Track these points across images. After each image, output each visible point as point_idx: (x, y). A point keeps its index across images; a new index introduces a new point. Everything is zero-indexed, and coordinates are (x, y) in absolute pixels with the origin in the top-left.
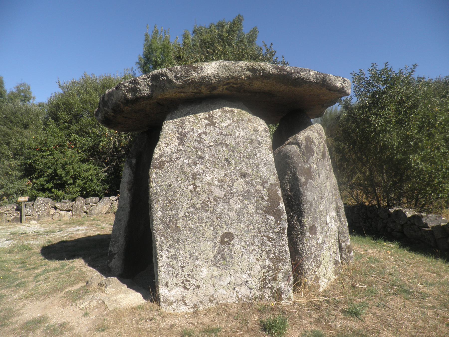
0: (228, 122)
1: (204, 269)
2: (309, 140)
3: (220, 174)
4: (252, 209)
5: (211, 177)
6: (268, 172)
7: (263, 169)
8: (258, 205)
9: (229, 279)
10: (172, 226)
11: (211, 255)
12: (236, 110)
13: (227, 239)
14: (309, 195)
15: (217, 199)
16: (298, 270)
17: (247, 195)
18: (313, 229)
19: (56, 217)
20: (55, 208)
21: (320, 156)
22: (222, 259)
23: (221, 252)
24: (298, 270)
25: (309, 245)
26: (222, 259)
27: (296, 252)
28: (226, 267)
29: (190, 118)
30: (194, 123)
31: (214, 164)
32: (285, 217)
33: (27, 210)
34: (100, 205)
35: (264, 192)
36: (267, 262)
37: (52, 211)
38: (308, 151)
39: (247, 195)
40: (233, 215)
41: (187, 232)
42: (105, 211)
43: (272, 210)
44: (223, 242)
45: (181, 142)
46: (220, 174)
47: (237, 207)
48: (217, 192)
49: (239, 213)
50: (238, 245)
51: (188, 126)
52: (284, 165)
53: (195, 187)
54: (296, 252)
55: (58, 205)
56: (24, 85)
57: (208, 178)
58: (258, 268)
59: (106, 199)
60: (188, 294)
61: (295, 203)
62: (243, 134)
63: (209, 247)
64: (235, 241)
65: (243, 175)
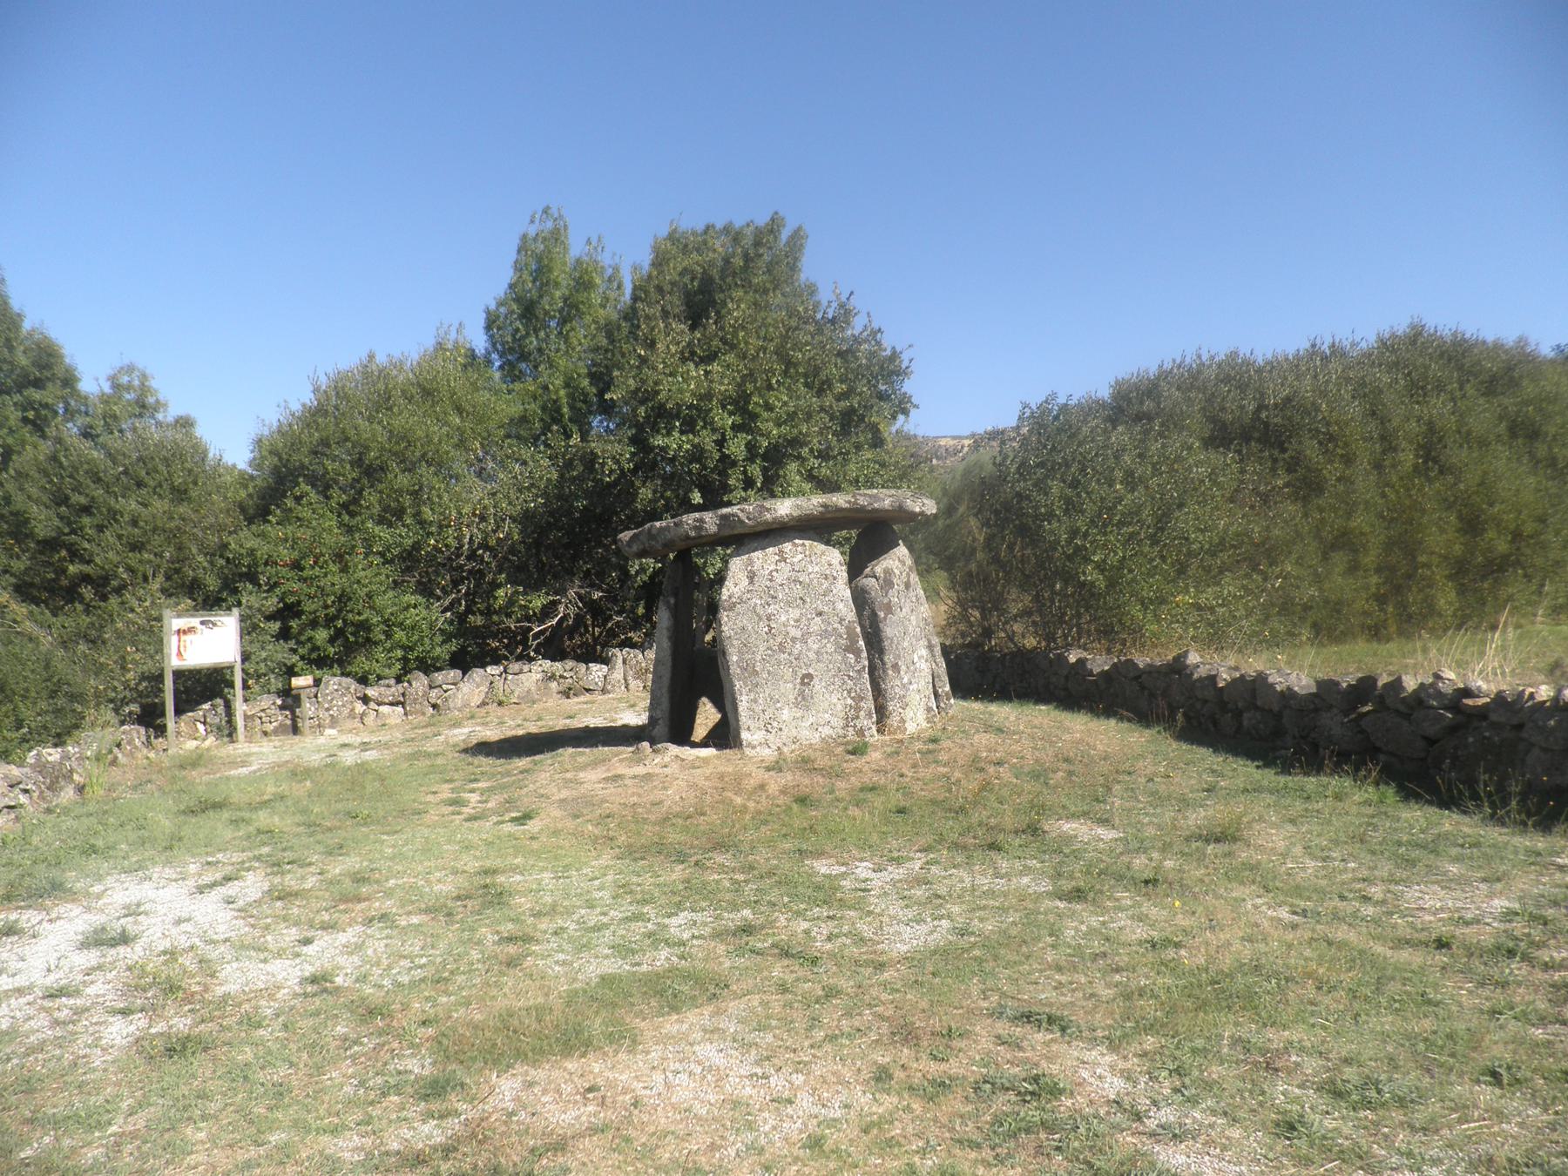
0: (800, 557)
1: (785, 711)
2: (888, 572)
3: (795, 613)
4: (830, 648)
5: (786, 617)
6: (847, 610)
7: (840, 606)
8: (836, 643)
9: (811, 720)
10: (750, 670)
11: (791, 697)
12: (807, 543)
13: (807, 679)
14: (889, 631)
15: (794, 640)
16: (881, 712)
17: (824, 634)
18: (896, 667)
19: (370, 719)
20: (365, 700)
21: (902, 587)
22: (803, 700)
23: (801, 693)
24: (881, 712)
25: (893, 685)
26: (803, 700)
27: (878, 692)
28: (808, 708)
29: (758, 554)
30: (764, 559)
31: (789, 604)
32: (864, 654)
33: (308, 708)
34: (466, 687)
35: (842, 630)
36: (849, 701)
37: (360, 707)
38: (888, 583)
39: (824, 634)
40: (812, 655)
41: (765, 675)
42: (477, 700)
43: (851, 648)
44: (803, 683)
45: (751, 581)
46: (795, 613)
47: (815, 647)
48: (794, 632)
49: (817, 653)
50: (818, 685)
51: (757, 565)
52: (861, 600)
53: (771, 629)
54: (878, 692)
55: (370, 692)
56: (130, 369)
57: (783, 619)
58: (839, 707)
59: (477, 674)
60: (771, 737)
61: (874, 640)
62: (817, 569)
63: (789, 689)
64: (816, 680)
65: (820, 614)
